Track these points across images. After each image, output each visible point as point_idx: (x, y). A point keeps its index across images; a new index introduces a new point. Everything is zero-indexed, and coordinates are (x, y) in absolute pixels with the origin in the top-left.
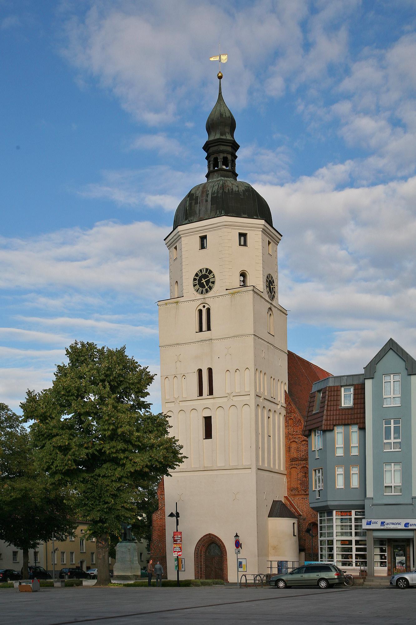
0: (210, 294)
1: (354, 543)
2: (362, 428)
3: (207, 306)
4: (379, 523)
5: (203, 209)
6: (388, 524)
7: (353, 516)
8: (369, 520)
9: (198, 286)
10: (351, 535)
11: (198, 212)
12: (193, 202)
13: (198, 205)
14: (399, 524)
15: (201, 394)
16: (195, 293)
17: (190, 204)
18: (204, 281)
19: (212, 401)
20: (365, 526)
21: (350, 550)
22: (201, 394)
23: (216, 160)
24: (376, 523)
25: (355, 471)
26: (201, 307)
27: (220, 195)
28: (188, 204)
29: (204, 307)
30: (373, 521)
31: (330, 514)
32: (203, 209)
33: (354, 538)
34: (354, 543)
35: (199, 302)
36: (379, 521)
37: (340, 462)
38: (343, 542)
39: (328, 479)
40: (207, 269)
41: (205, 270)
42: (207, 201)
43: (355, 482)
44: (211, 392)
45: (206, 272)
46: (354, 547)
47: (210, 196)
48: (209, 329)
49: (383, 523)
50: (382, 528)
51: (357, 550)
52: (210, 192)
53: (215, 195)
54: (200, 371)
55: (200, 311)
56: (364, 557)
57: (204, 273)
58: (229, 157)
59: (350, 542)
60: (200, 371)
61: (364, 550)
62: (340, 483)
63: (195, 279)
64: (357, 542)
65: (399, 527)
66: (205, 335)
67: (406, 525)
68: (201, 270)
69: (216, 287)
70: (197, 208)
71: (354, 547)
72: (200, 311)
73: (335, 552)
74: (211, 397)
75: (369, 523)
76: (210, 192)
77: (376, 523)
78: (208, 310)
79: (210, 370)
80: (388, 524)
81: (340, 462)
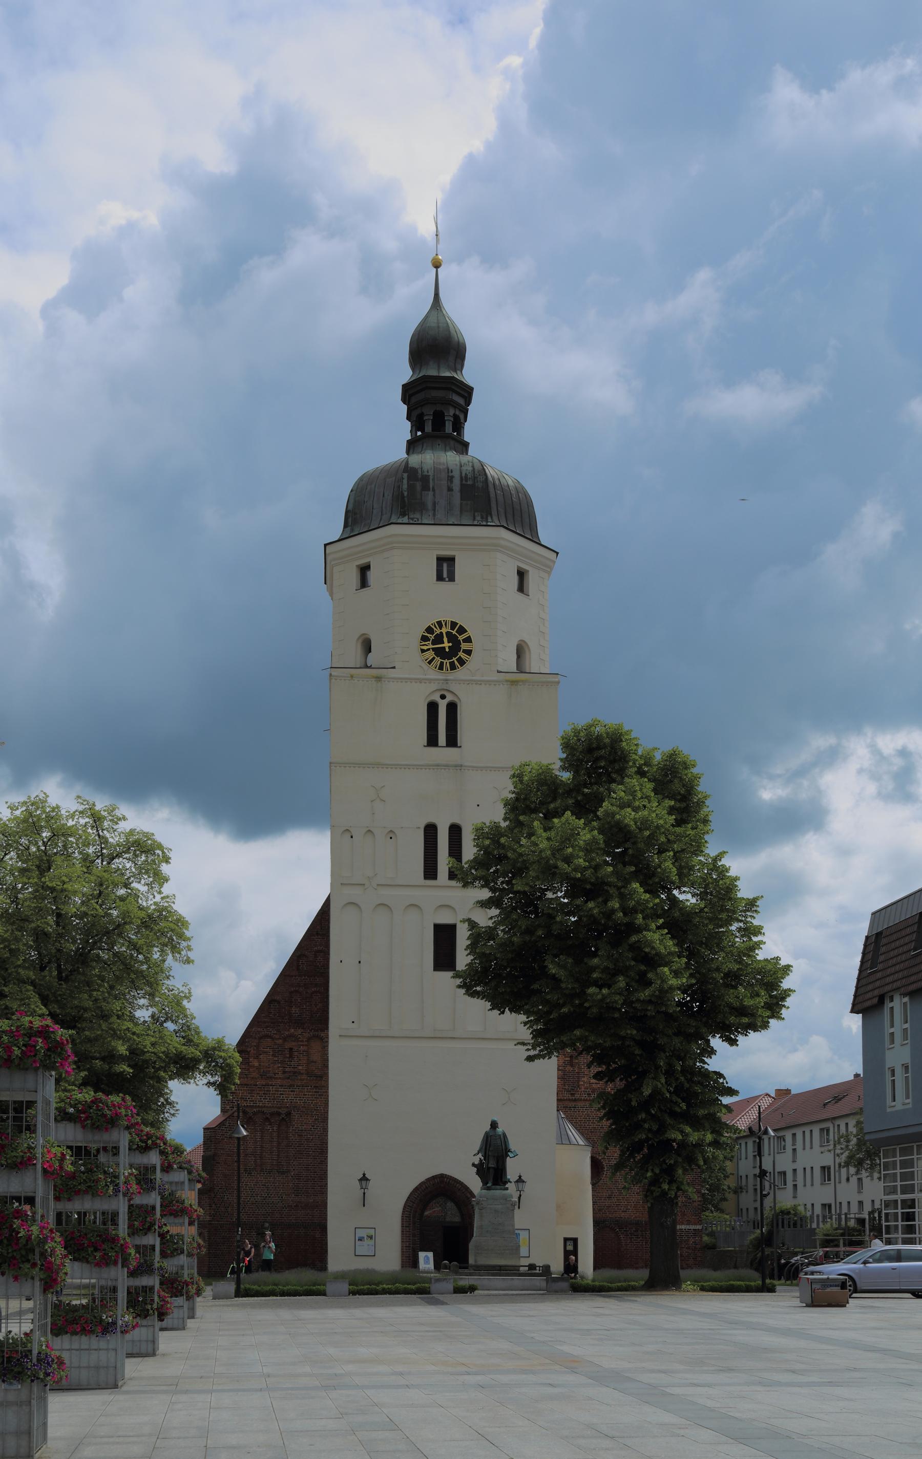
0: (461, 673)
11: (430, 505)
12: (418, 485)
13: (431, 493)
16: (425, 666)
17: (411, 488)
18: (446, 645)
26: (436, 697)
27: (480, 485)
28: (405, 486)
29: (443, 697)
35: (434, 686)
41: (449, 625)
42: (450, 489)
52: (456, 474)
53: (470, 482)
55: (432, 708)
58: (462, 417)
60: (431, 831)
66: (442, 754)
69: (473, 663)
70: (429, 497)
76: (456, 474)
78: (452, 708)
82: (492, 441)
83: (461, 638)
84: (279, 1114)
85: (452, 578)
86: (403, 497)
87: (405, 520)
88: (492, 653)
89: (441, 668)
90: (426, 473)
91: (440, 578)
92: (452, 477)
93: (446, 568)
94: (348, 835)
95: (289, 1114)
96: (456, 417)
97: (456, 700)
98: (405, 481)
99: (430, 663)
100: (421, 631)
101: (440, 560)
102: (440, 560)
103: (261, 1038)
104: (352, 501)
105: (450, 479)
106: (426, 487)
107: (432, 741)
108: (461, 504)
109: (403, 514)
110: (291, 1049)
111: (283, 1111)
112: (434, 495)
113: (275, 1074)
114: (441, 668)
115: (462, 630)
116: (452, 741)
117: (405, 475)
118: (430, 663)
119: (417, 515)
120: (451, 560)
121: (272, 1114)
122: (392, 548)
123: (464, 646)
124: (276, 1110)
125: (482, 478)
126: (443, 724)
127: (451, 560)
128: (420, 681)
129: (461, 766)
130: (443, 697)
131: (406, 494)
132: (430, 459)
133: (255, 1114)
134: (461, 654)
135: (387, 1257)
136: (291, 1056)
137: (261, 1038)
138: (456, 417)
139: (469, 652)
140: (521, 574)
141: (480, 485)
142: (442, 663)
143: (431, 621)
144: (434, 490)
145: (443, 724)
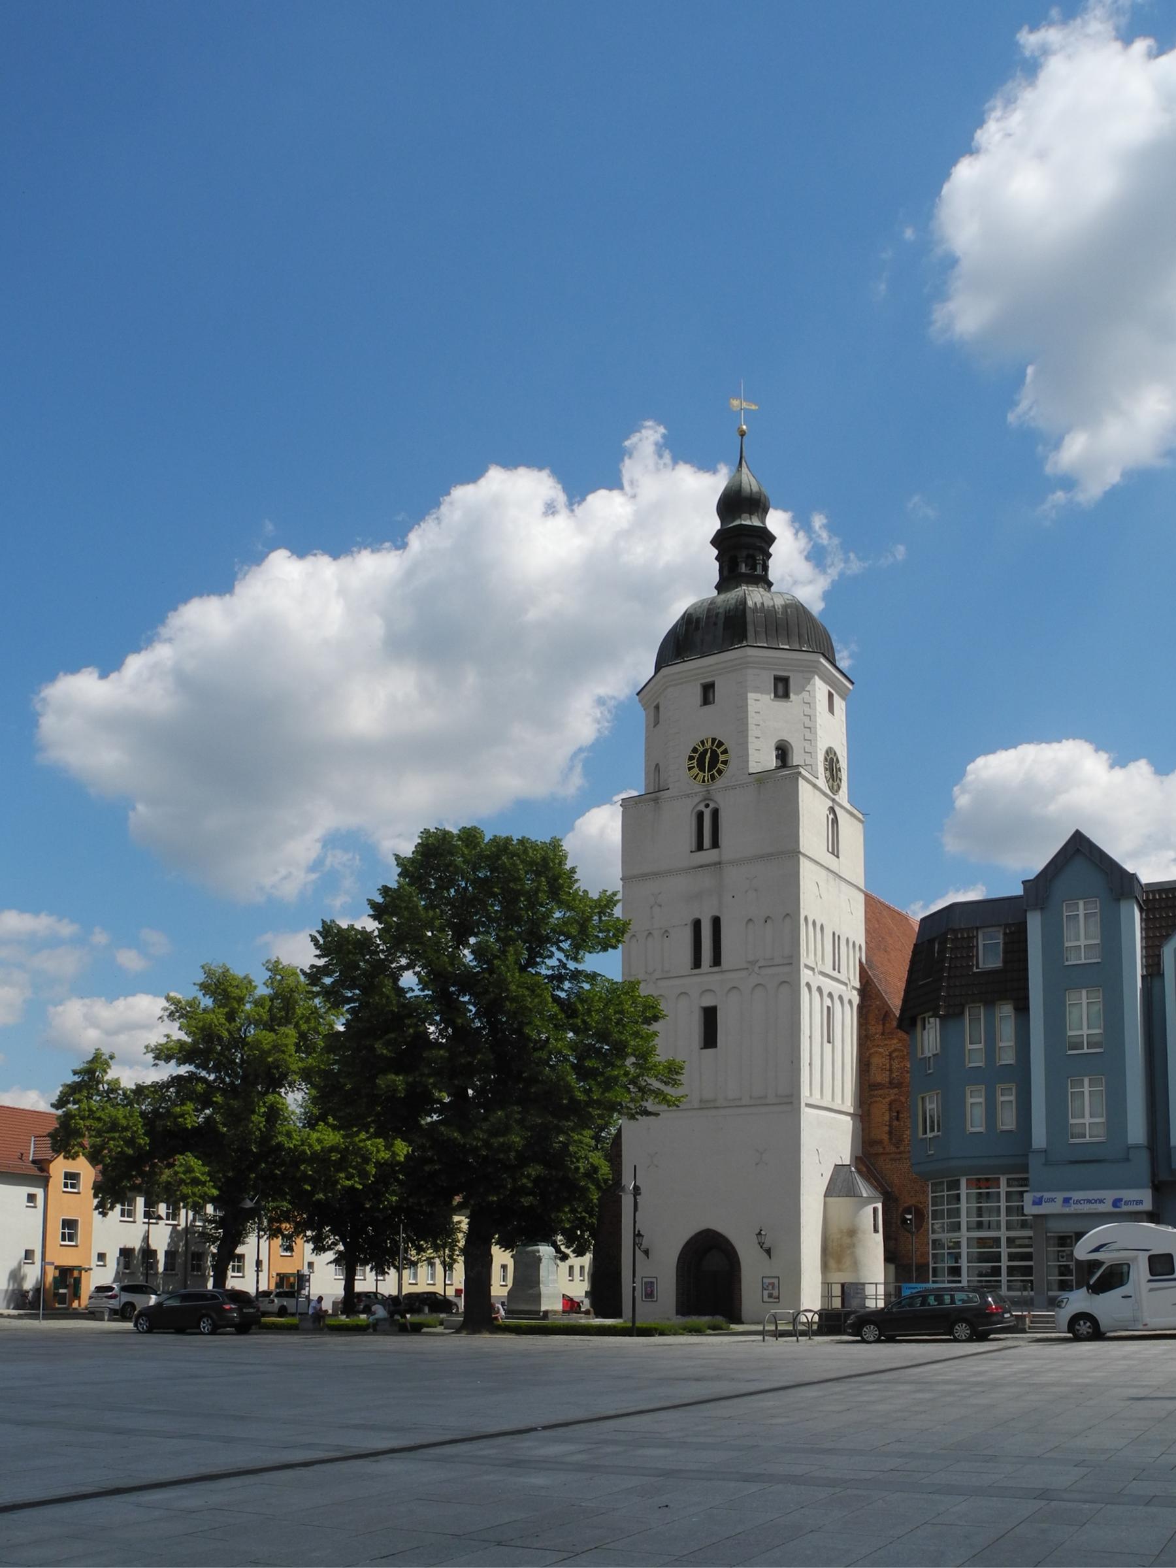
0: (720, 782)
1: (1004, 1242)
2: (1022, 1008)
3: (712, 805)
4: (1060, 1200)
6: (1078, 1202)
7: (1003, 1188)
8: (1038, 1195)
9: (696, 770)
10: (999, 1228)
14: (1101, 1201)
15: (697, 964)
19: (717, 977)
20: (1030, 1210)
21: (997, 1257)
22: (697, 964)
24: (1053, 1200)
25: (1007, 1098)
26: (702, 807)
29: (707, 806)
30: (1047, 1195)
31: (955, 1185)
33: (1003, 1234)
34: (1004, 1242)
35: (697, 800)
36: (1060, 1196)
37: (976, 1077)
38: (982, 1242)
39: (953, 1109)
40: (714, 740)
43: (1008, 1121)
44: (717, 961)
46: (1004, 1251)
48: (715, 844)
49: (1066, 1201)
50: (1067, 1210)
51: (1012, 1257)
54: (697, 924)
55: (700, 816)
56: (1028, 1271)
59: (997, 1241)
60: (697, 924)
61: (1028, 1256)
62: (976, 1122)
63: (691, 758)
64: (1011, 1241)
65: (1101, 1208)
66: (709, 856)
67: (1116, 1203)
69: (730, 771)
71: (1004, 1251)
72: (700, 816)
73: (964, 1263)
74: (716, 969)
75: (1038, 1202)
77: (1053, 1200)
78: (715, 814)
79: (716, 922)
80: (1078, 1202)
81: (976, 1077)
83: (719, 751)
100: (688, 752)
106: (697, 628)
107: (700, 847)
114: (704, 781)
115: (720, 744)
123: (722, 758)
129: (720, 863)
130: (707, 806)
134: (720, 765)
139: (725, 762)
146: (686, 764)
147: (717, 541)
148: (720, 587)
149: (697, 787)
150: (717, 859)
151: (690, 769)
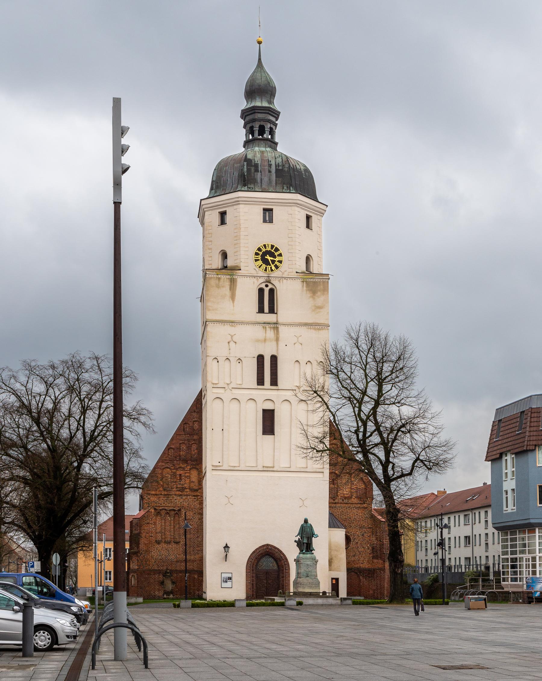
0: (277, 273)
3: (270, 286)
5: (266, 179)
9: (260, 262)
12: (253, 169)
13: (259, 173)
17: (249, 170)
19: (275, 393)
23: (252, 128)
26: (263, 286)
27: (286, 169)
28: (245, 170)
29: (267, 286)
32: (266, 179)
35: (262, 280)
40: (272, 246)
41: (270, 246)
42: (270, 172)
45: (272, 248)
47: (273, 167)
52: (273, 163)
53: (280, 168)
57: (269, 249)
60: (260, 359)
68: (265, 246)
69: (283, 267)
78: (272, 292)
79: (274, 359)
82: (291, 142)
84: (174, 510)
85: (271, 221)
86: (244, 175)
87: (246, 188)
88: (292, 262)
89: (266, 270)
90: (256, 162)
91: (265, 221)
92: (271, 165)
93: (268, 215)
94: (216, 361)
95: (180, 510)
96: (271, 129)
97: (274, 287)
98: (245, 167)
99: (260, 267)
101: (265, 210)
102: (265, 210)
103: (164, 469)
104: (215, 175)
105: (270, 166)
106: (257, 170)
107: (261, 310)
108: (276, 180)
109: (245, 185)
110: (180, 475)
111: (177, 509)
112: (261, 175)
113: (172, 488)
114: (266, 270)
115: (277, 250)
116: (272, 310)
117: (245, 163)
118: (260, 267)
119: (252, 186)
120: (271, 210)
121: (170, 510)
122: (239, 204)
124: (173, 508)
125: (287, 166)
126: (267, 300)
127: (271, 210)
128: (254, 277)
130: (267, 286)
131: (246, 174)
132: (257, 152)
133: (161, 510)
135: (238, 591)
136: (180, 479)
137: (164, 469)
138: (271, 129)
139: (280, 262)
140: (308, 218)
141: (286, 169)
142: (266, 268)
143: (260, 245)
144: (261, 172)
145: (267, 300)
146: (253, 257)
147: (245, 114)
148: (247, 144)
149: (261, 273)
150: (275, 321)
151: (256, 260)
